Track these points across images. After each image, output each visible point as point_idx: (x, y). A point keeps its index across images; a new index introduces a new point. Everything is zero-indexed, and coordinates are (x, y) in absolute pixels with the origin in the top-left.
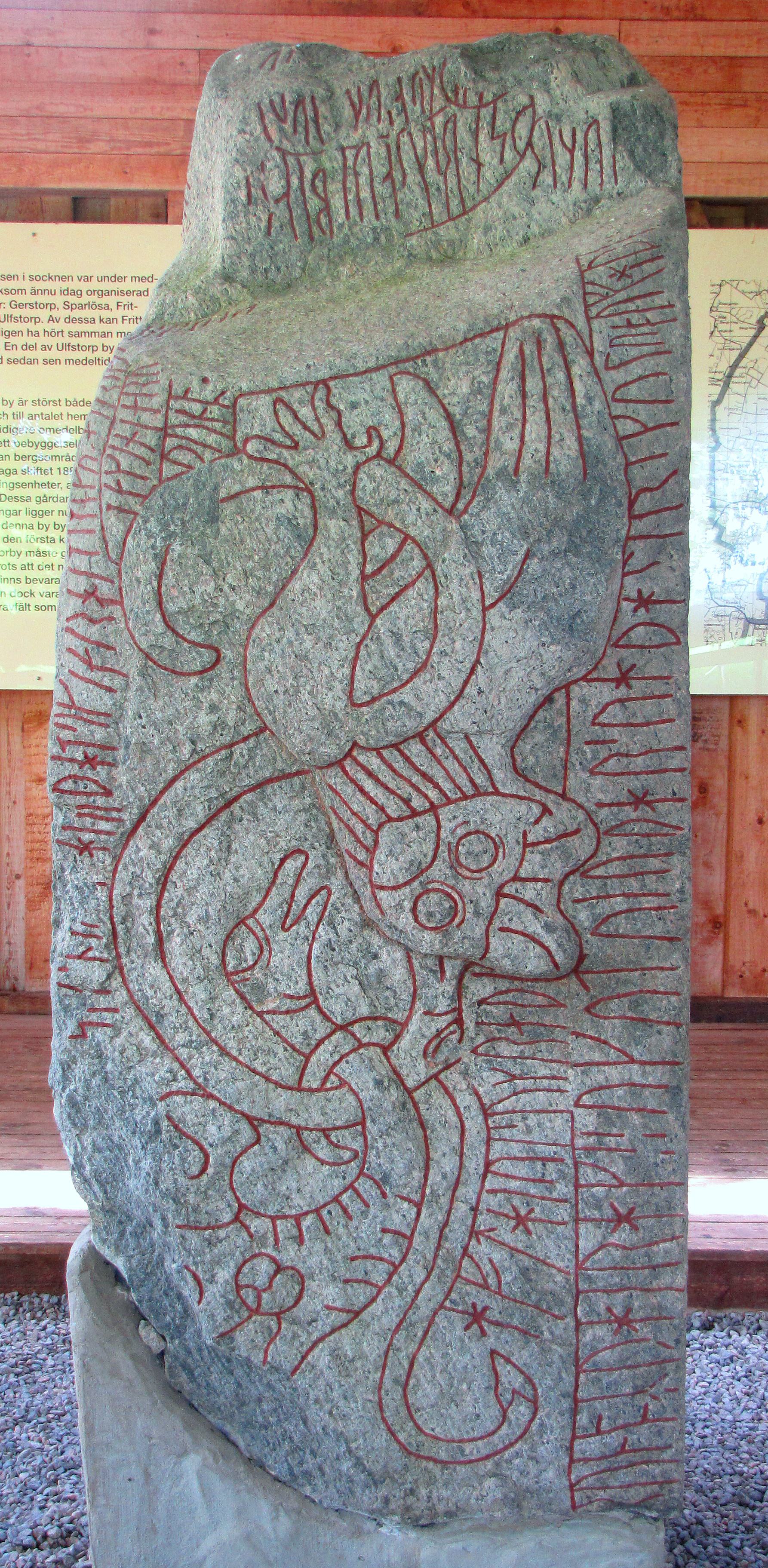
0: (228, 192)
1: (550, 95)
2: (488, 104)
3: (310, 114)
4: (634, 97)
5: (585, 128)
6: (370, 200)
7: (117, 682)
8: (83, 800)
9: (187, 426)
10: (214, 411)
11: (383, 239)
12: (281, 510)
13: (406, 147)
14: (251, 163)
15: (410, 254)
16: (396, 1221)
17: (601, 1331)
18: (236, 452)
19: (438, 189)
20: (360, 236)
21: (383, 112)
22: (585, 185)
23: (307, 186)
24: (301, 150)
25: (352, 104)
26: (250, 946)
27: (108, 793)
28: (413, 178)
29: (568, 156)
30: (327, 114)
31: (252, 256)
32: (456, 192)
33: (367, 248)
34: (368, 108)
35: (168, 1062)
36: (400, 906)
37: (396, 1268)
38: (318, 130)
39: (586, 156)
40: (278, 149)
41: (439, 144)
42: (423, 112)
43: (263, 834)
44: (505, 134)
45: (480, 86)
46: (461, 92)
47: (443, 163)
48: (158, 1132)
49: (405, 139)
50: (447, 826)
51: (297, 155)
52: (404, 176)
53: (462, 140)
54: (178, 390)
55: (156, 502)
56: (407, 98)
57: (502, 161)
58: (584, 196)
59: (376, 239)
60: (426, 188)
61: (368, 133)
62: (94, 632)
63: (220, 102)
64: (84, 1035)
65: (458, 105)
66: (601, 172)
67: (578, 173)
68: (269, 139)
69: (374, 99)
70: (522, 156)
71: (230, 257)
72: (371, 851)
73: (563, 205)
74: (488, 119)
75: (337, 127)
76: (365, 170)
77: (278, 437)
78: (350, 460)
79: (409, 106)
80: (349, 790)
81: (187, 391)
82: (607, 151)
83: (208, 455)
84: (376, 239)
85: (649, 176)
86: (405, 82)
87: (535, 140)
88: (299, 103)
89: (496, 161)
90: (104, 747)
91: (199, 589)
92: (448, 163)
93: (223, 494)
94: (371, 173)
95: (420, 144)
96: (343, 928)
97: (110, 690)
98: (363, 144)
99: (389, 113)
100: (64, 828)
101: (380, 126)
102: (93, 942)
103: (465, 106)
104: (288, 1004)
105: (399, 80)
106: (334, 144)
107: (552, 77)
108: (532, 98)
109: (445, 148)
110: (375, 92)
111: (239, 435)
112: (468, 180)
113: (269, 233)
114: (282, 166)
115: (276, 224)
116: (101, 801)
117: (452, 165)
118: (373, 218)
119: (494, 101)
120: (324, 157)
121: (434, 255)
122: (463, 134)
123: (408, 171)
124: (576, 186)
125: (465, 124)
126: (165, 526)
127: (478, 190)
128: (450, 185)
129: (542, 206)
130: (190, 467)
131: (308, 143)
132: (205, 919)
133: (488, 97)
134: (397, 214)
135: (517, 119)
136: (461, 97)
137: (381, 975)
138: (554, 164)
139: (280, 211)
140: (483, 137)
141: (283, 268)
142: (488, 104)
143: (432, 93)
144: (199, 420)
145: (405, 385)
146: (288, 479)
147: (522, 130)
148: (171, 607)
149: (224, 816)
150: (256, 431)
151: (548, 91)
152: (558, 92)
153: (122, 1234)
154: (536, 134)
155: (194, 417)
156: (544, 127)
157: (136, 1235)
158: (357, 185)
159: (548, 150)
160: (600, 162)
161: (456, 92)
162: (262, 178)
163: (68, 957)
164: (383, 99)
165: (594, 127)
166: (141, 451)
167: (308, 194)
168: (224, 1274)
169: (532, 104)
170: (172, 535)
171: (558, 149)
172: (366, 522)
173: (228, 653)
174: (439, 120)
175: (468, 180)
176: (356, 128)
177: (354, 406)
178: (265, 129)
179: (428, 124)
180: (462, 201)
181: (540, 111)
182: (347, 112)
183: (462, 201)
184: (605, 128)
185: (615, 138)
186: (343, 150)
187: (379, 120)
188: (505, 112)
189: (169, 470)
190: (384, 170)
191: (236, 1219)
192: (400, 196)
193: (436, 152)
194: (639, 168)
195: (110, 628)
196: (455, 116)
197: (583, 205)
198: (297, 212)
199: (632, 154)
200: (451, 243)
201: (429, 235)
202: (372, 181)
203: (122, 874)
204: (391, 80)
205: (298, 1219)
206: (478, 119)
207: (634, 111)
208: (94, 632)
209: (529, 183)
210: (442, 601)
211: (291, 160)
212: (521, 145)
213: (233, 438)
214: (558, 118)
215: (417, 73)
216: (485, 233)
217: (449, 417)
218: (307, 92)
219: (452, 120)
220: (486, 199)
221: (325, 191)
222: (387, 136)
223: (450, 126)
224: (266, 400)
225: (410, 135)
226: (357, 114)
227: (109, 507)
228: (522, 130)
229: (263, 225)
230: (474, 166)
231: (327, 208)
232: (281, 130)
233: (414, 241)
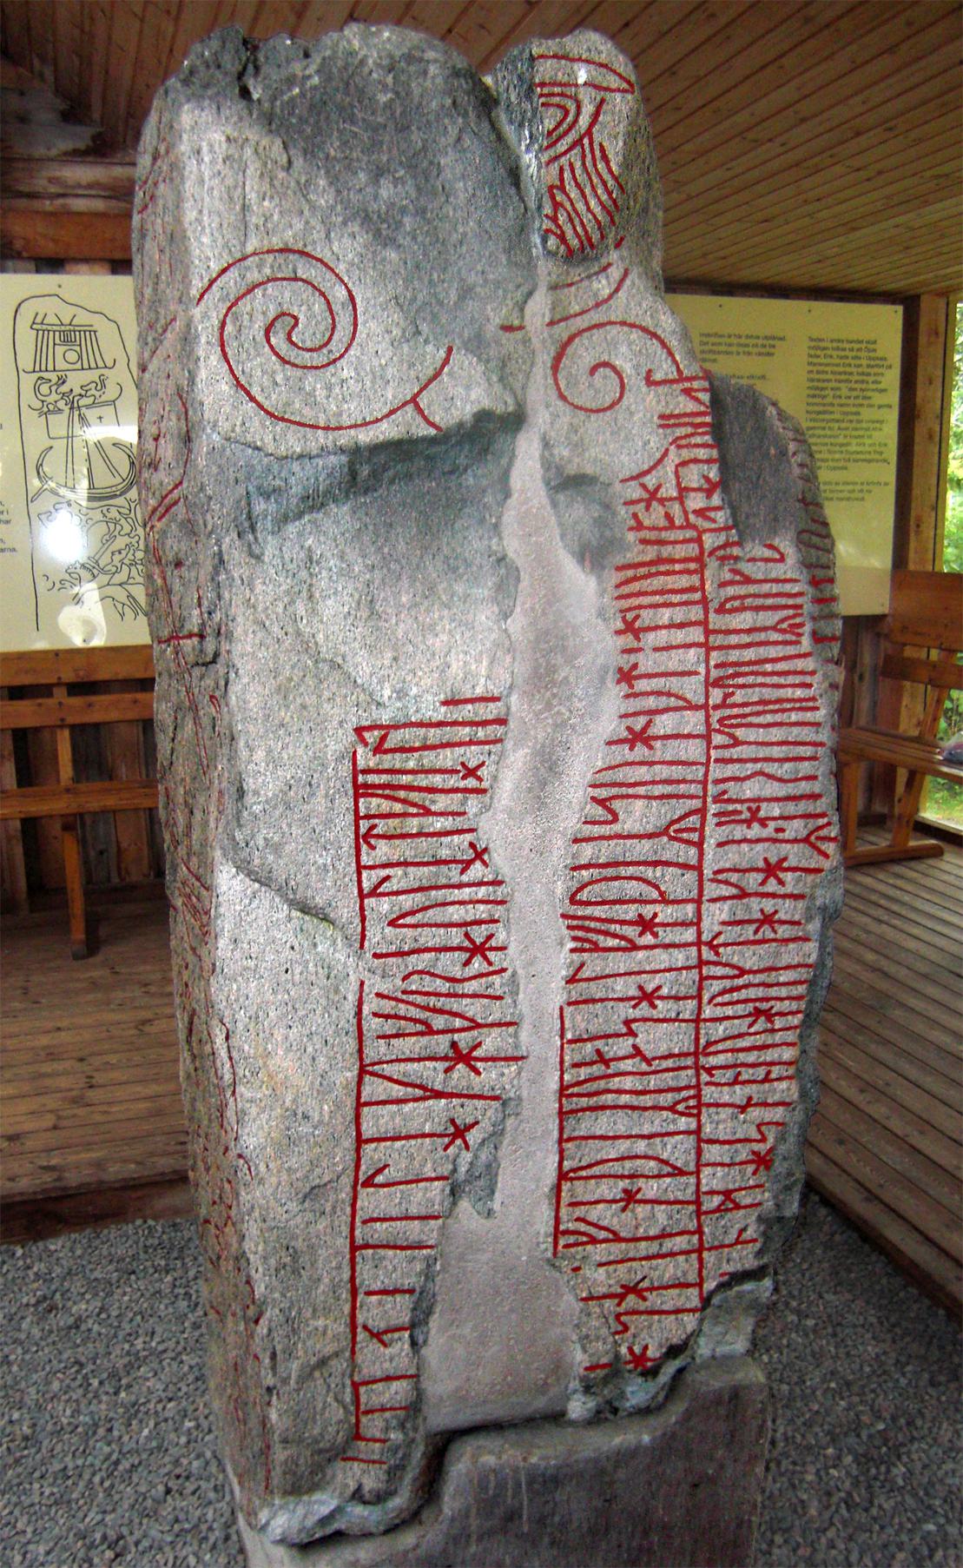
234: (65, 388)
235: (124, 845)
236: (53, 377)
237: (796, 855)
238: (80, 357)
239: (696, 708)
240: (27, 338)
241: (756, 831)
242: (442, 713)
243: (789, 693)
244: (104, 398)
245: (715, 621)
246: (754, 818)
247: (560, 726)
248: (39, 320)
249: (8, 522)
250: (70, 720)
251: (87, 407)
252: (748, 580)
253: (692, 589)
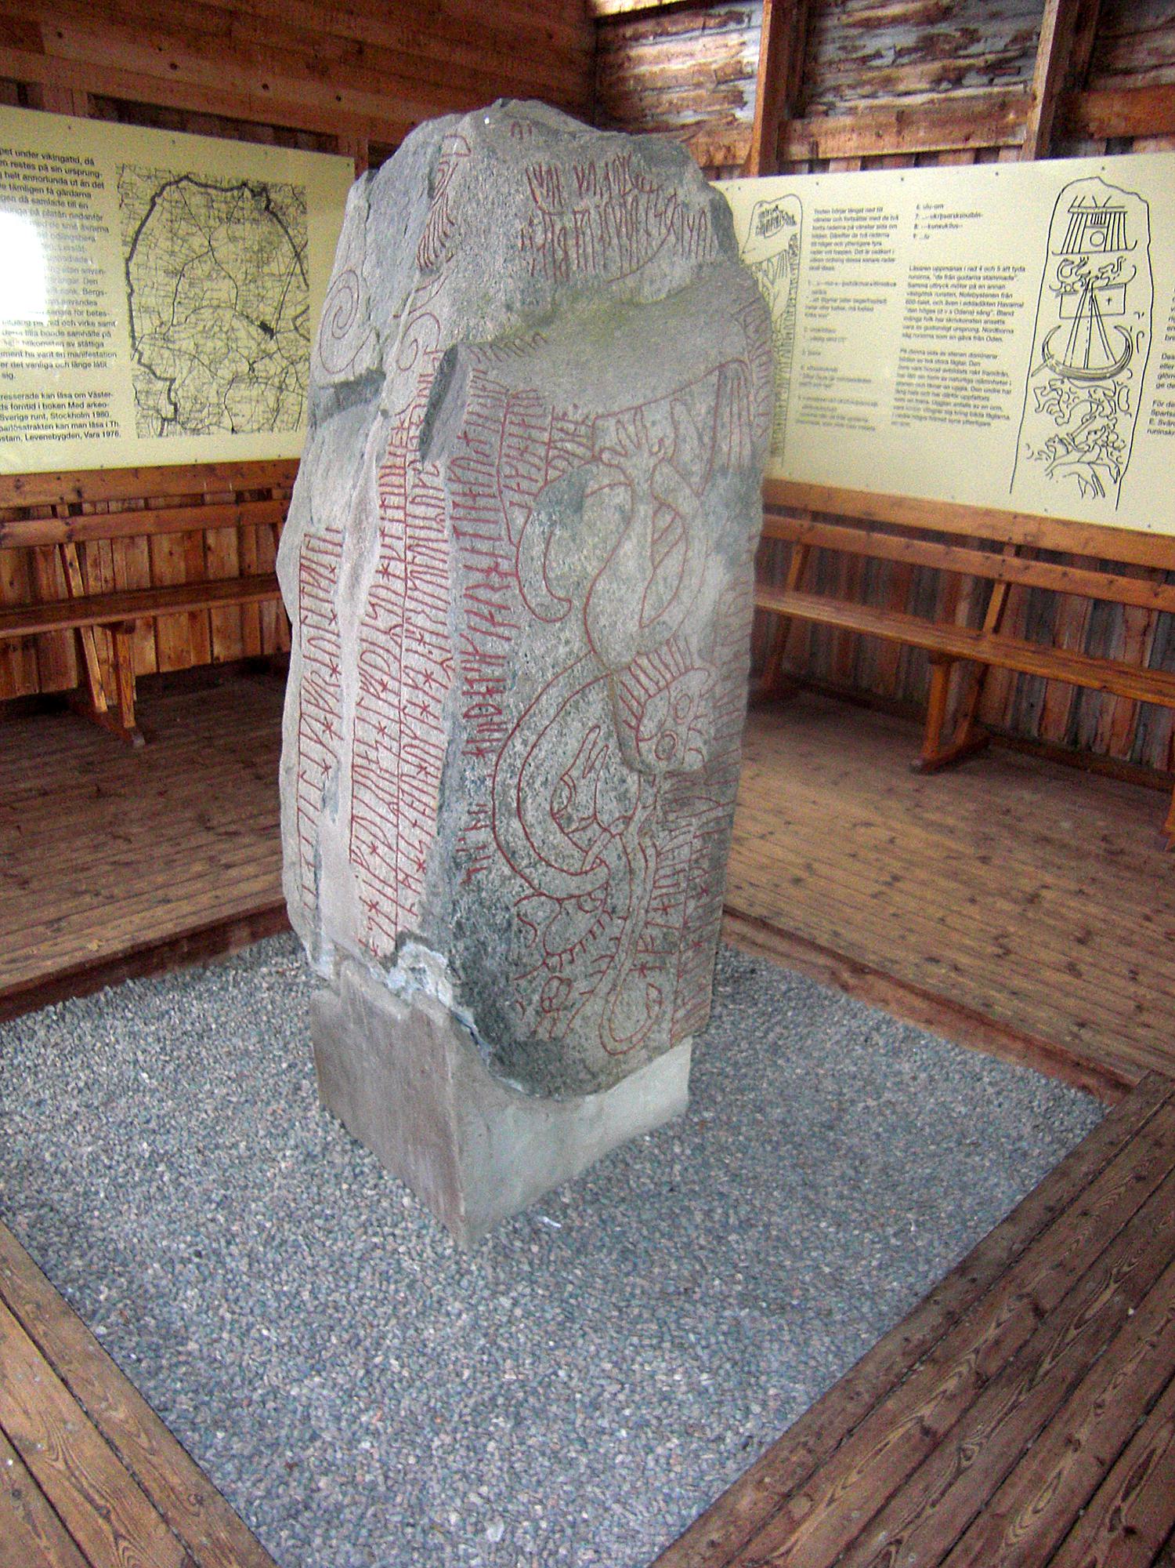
7: (514, 632)
8: (481, 720)
9: (562, 440)
10: (583, 430)
12: (617, 501)
14: (525, 219)
16: (617, 932)
17: (690, 953)
18: (596, 459)
26: (566, 793)
27: (500, 712)
28: (615, 241)
35: (519, 881)
36: (650, 751)
37: (612, 957)
43: (581, 721)
48: (510, 924)
50: (673, 694)
51: (550, 214)
54: (559, 412)
55: (542, 498)
62: (496, 598)
63: (493, 162)
64: (469, 878)
72: (639, 719)
77: (619, 448)
78: (652, 462)
80: (633, 682)
81: (565, 414)
83: (576, 463)
88: (549, 172)
90: (498, 680)
91: (568, 561)
93: (589, 490)
96: (612, 770)
97: (508, 639)
100: (468, 742)
102: (482, 816)
103: (642, 190)
104: (584, 823)
111: (597, 448)
116: (496, 719)
126: (550, 519)
130: (563, 471)
132: (545, 783)
133: (655, 187)
137: (627, 791)
140: (651, 213)
144: (573, 436)
145: (679, 408)
146: (622, 478)
148: (551, 575)
149: (563, 713)
150: (608, 445)
153: (471, 995)
155: (567, 433)
157: (479, 993)
163: (466, 830)
166: (536, 461)
168: (536, 998)
170: (553, 524)
172: (662, 505)
173: (576, 603)
174: (630, 199)
177: (654, 423)
184: (709, 215)
186: (575, 213)
189: (553, 474)
191: (544, 963)
195: (509, 594)
203: (503, 765)
205: (571, 950)
208: (496, 598)
210: (690, 554)
213: (592, 449)
217: (697, 429)
219: (636, 200)
220: (650, 260)
224: (612, 421)
227: (512, 504)
234: (1084, 270)
235: (1050, 704)
236: (1076, 259)
237: (438, 673)
238: (1105, 239)
239: (400, 560)
240: (1063, 220)
241: (420, 649)
242: (323, 533)
243: (436, 564)
244: (1118, 280)
245: (410, 508)
246: (421, 641)
247: (361, 555)
248: (1076, 204)
249: (1008, 392)
250: (1007, 577)
251: (1101, 289)
252: (424, 486)
253: (400, 486)
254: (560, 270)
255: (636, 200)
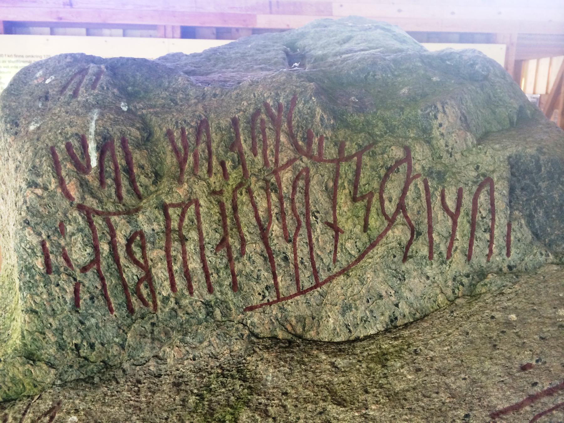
0: (21, 258)
1: (432, 148)
2: (350, 157)
3: (121, 162)
4: (540, 150)
5: (475, 188)
6: (200, 271)
11: (217, 312)
13: (245, 209)
15: (252, 334)
19: (286, 259)
20: (190, 310)
21: (215, 162)
22: (469, 258)
23: (122, 253)
24: (111, 208)
25: (176, 150)
28: (254, 247)
29: (450, 223)
30: (143, 162)
31: (59, 331)
32: (308, 264)
33: (200, 323)
34: (195, 156)
38: (132, 182)
39: (473, 224)
40: (80, 207)
41: (287, 205)
42: (266, 163)
44: (371, 194)
45: (341, 134)
46: (316, 140)
47: (291, 229)
49: (244, 198)
51: (106, 216)
52: (243, 242)
53: (316, 202)
56: (245, 147)
57: (366, 228)
58: (467, 269)
59: (210, 314)
60: (269, 257)
61: (196, 188)
65: (310, 157)
66: (491, 242)
67: (461, 242)
68: (68, 195)
69: (203, 146)
70: (391, 221)
71: (30, 333)
73: (440, 279)
74: (350, 176)
75: (157, 177)
76: (193, 235)
79: (248, 156)
82: (501, 220)
84: (210, 314)
85: (549, 246)
86: (242, 125)
87: (409, 202)
89: (358, 229)
92: (298, 229)
94: (201, 239)
95: (262, 205)
98: (190, 201)
99: (223, 164)
101: (212, 180)
103: (319, 159)
105: (235, 122)
106: (153, 200)
107: (436, 123)
108: (407, 150)
109: (293, 209)
110: (204, 138)
112: (323, 249)
113: (76, 304)
114: (87, 230)
115: (85, 297)
117: (303, 231)
118: (205, 291)
119: (359, 154)
120: (141, 218)
121: (281, 334)
122: (318, 195)
123: (248, 237)
124: (458, 257)
125: (320, 183)
127: (335, 260)
128: (299, 254)
129: (416, 283)
131: (120, 197)
133: (351, 148)
134: (235, 287)
135: (387, 176)
136: (315, 147)
138: (430, 232)
139: (90, 280)
140: (343, 197)
141: (98, 346)
142: (350, 157)
143: (278, 141)
147: (393, 190)
151: (428, 142)
152: (442, 142)
154: (410, 194)
156: (421, 187)
158: (184, 253)
159: (425, 214)
160: (490, 230)
161: (308, 140)
162: (63, 242)
164: (214, 145)
165: (487, 188)
167: (123, 261)
169: (408, 158)
171: (438, 213)
174: (287, 176)
175: (323, 249)
176: (180, 182)
178: (61, 183)
179: (273, 180)
180: (315, 273)
181: (417, 167)
182: (170, 160)
183: (315, 273)
184: (501, 188)
185: (510, 205)
186: (164, 208)
187: (209, 171)
188: (372, 168)
190: (218, 236)
192: (238, 266)
193: (282, 214)
194: (536, 236)
196: (307, 170)
197: (465, 280)
198: (112, 281)
199: (530, 219)
200: (301, 319)
201: (274, 310)
202: (202, 248)
204: (225, 122)
206: (336, 176)
207: (539, 168)
209: (400, 256)
211: (98, 221)
212: (390, 208)
214: (441, 177)
215: (258, 112)
216: (343, 315)
218: (115, 132)
219: (302, 176)
221: (144, 256)
222: (221, 192)
223: (301, 183)
225: (249, 192)
226: (182, 163)
228: (393, 190)
229: (69, 297)
230: (331, 233)
231: (148, 279)
232: (83, 185)
233: (255, 318)
254: (136, 298)
255: (302, 176)
